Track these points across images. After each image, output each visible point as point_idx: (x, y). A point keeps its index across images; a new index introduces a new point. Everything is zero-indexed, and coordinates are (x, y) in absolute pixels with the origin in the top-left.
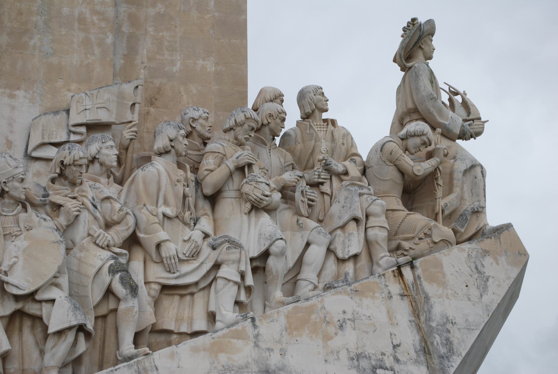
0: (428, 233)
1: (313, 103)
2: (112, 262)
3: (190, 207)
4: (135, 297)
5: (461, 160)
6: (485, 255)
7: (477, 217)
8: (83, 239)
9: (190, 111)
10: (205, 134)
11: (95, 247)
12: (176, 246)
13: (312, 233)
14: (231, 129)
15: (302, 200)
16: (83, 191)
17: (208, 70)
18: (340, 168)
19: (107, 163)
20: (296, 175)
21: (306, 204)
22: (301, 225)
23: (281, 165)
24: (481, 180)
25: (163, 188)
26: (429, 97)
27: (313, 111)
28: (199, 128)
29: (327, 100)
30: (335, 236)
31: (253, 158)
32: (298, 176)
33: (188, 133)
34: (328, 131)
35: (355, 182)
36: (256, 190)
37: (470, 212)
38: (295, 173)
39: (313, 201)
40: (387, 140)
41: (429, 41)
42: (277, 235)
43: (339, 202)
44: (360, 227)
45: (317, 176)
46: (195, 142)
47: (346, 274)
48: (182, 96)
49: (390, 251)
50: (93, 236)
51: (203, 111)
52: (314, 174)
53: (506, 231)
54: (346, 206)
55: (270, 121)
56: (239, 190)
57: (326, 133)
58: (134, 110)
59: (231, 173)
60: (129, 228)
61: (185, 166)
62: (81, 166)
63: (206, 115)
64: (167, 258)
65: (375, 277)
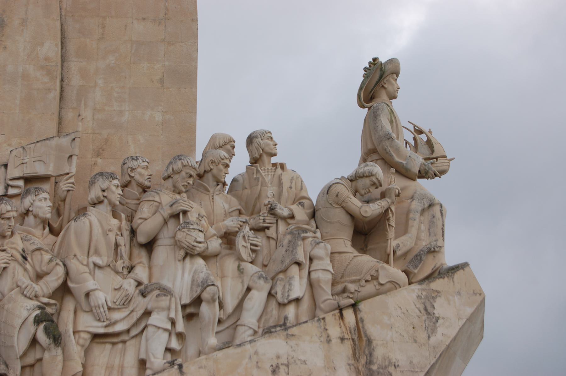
0: (375, 275)
1: (260, 147)
2: (38, 312)
3: (123, 256)
4: (58, 347)
5: (419, 199)
6: (436, 296)
7: (434, 256)
8: (12, 290)
9: (129, 161)
10: (144, 183)
11: (23, 298)
12: (106, 295)
13: (252, 278)
14: (169, 177)
15: (243, 246)
16: (13, 243)
17: (157, 119)
18: (285, 213)
19: (41, 215)
20: (239, 221)
21: (248, 249)
22: (242, 270)
23: (225, 211)
24: (439, 219)
25: (94, 238)
26: (386, 137)
27: (261, 156)
28: (137, 177)
29: (276, 145)
30: (277, 281)
31: (188, 205)
32: (241, 222)
33: (127, 183)
34: (275, 176)
35: (301, 226)
36: (188, 237)
37: (426, 252)
38: (238, 218)
39: (256, 246)
40: (334, 182)
41: (392, 81)
42: (209, 281)
43: (283, 246)
44: (303, 271)
45: (262, 221)
46: (133, 191)
47: (286, 318)
48: (130, 145)
49: (332, 295)
50: (21, 287)
51: (142, 160)
52: (259, 219)
53: (462, 270)
54: (289, 249)
55: (212, 167)
56: (174, 237)
57: (273, 177)
58: (71, 162)
59: (165, 220)
60: (59, 278)
61: (121, 216)
62: (9, 219)
63: (146, 164)
64: (96, 307)
65: (314, 321)
